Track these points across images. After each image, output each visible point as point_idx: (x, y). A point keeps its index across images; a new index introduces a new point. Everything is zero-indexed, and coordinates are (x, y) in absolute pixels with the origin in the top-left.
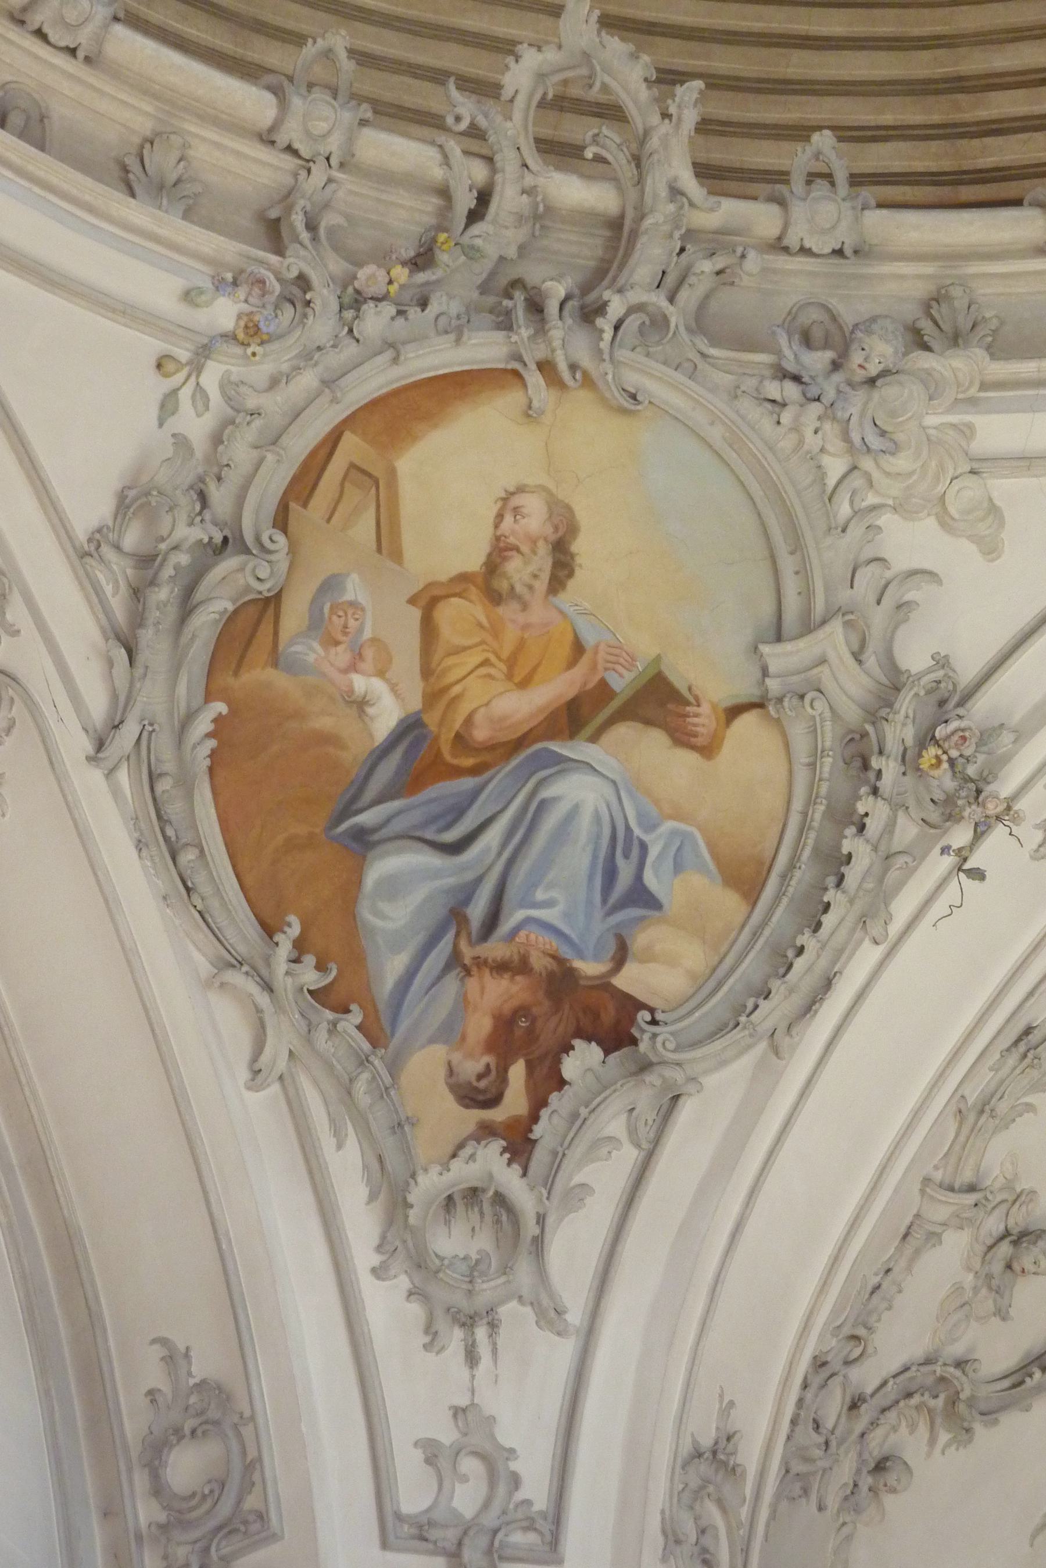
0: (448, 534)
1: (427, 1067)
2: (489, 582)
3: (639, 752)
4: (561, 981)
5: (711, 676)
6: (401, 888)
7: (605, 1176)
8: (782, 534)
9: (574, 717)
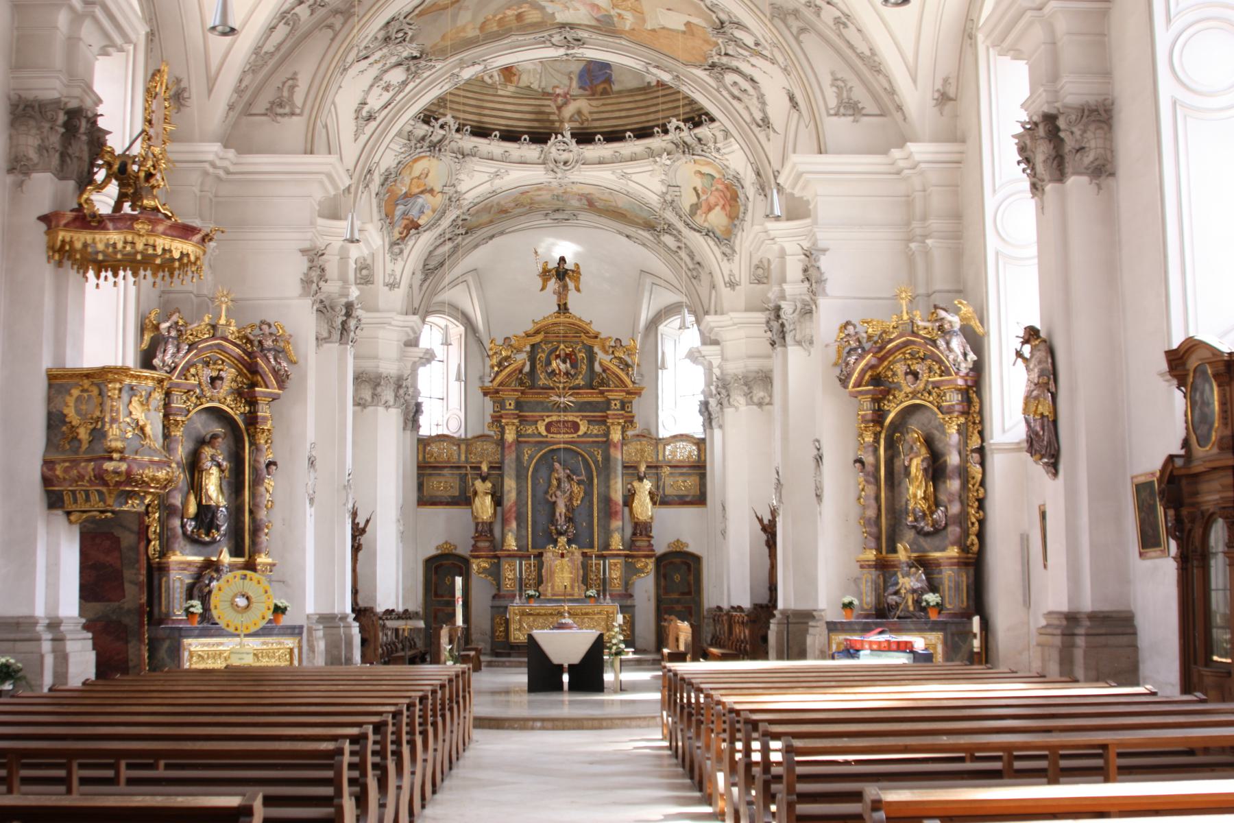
0: (416, 173)
1: (397, 230)
2: (418, 178)
3: (428, 196)
4: (412, 221)
5: (437, 188)
6: (400, 209)
7: (411, 243)
8: (450, 174)
9: (422, 192)
